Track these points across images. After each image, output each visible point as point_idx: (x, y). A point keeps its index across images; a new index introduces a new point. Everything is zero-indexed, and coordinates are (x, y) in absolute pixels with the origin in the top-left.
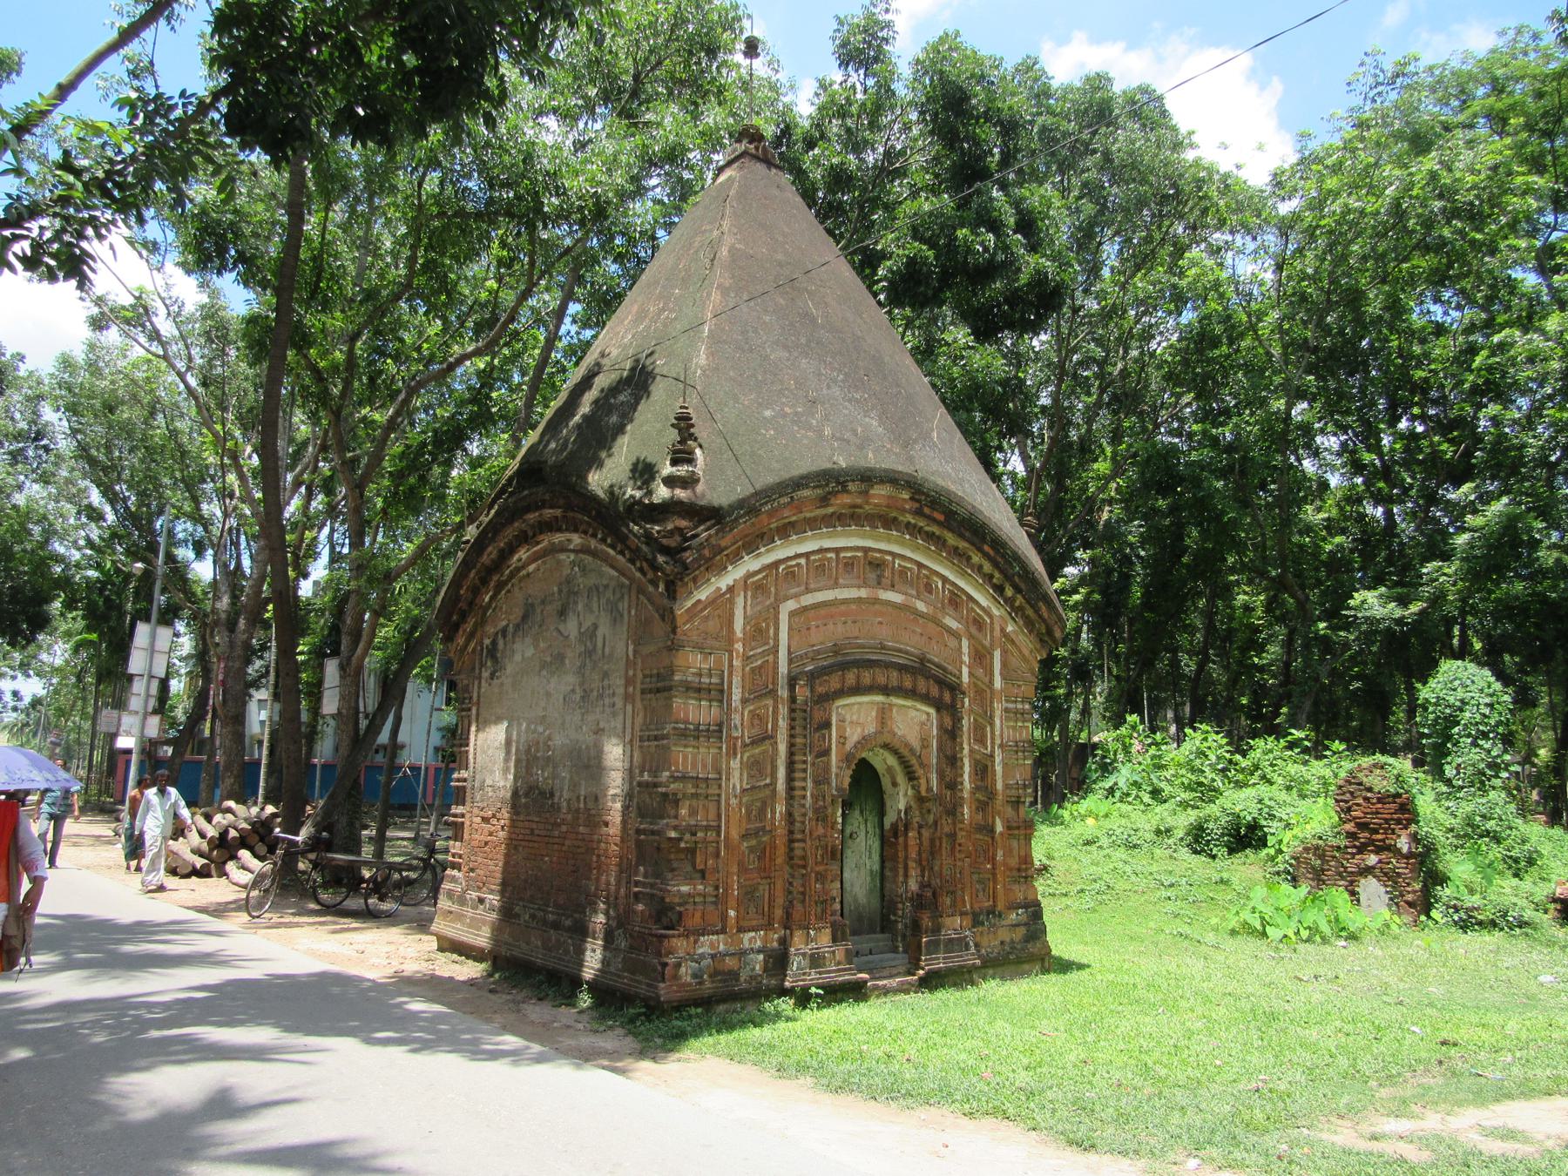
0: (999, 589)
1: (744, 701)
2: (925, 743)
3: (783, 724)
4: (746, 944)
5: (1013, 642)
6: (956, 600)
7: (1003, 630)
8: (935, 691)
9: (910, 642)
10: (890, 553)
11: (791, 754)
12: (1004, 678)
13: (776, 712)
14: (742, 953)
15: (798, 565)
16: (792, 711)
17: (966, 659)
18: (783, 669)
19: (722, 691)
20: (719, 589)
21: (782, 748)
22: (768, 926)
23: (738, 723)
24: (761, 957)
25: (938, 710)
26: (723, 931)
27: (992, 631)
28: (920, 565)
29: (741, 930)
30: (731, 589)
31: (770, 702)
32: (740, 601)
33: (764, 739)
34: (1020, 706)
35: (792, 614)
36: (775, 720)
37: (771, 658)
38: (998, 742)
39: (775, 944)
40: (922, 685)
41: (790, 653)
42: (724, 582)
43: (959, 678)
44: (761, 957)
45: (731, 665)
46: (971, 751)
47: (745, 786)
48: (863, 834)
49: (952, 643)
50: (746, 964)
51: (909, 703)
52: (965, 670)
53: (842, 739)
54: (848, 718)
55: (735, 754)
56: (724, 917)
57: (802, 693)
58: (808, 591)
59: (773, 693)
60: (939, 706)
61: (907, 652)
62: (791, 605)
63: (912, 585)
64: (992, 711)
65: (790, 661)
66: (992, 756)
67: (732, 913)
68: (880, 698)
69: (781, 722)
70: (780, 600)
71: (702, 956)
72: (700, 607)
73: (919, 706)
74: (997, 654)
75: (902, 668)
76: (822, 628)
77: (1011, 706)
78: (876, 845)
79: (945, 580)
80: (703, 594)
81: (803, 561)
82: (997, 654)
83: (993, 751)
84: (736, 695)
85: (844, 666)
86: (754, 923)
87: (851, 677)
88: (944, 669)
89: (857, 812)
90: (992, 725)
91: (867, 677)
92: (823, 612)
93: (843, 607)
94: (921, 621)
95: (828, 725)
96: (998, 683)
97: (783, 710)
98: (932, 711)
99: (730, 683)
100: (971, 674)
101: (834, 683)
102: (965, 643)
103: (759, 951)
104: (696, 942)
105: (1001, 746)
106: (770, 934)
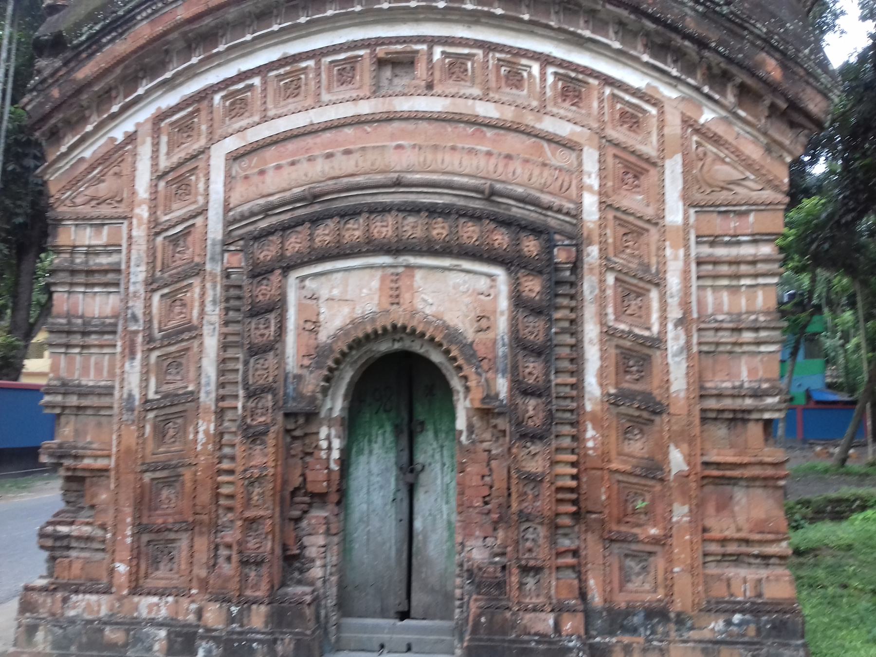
0: (661, 49)
1: (152, 284)
2: (483, 321)
3: (214, 314)
4: (144, 613)
5: (716, 140)
6: (573, 85)
7: (688, 122)
8: (501, 239)
9: (466, 163)
10: (420, 40)
11: (224, 346)
12: (689, 203)
13: (203, 295)
14: (133, 625)
15: (250, 87)
16: (227, 288)
17: (593, 181)
18: (215, 229)
19: (118, 271)
20: (113, 139)
21: (211, 343)
22: (179, 592)
23: (139, 311)
24: (163, 633)
25: (508, 269)
26: (107, 591)
27: (661, 128)
28: (488, 47)
29: (136, 590)
30: (131, 138)
31: (196, 281)
32: (145, 150)
33: (189, 329)
34: (747, 251)
35: (235, 157)
36: (202, 304)
37: (199, 221)
38: (675, 313)
39: (191, 618)
40: (470, 233)
41: (227, 209)
42: (118, 134)
43: (576, 215)
44: (163, 633)
45: (130, 237)
46: (608, 333)
47: (151, 395)
48: (438, 466)
49: (561, 158)
50: (138, 640)
51: (447, 262)
52: (590, 204)
53: (312, 326)
54: (324, 293)
55: (132, 355)
56: (112, 571)
57: (236, 260)
58: (265, 119)
59: (198, 270)
60: (510, 261)
61: (449, 186)
62: (232, 144)
63: (473, 83)
64: (663, 262)
65: (228, 223)
66: (658, 343)
67: (122, 568)
68: (386, 260)
69: (209, 308)
70: (212, 140)
71: (72, 621)
72: (84, 166)
73: (467, 265)
74: (673, 167)
75: (433, 211)
76: (287, 170)
77: (706, 250)
78: (453, 484)
79: (546, 60)
80: (88, 152)
81: (257, 81)
82: (673, 167)
83: (663, 331)
84: (139, 274)
85: (315, 220)
86: (162, 584)
87: (324, 234)
88: (536, 203)
89: (430, 434)
90: (659, 282)
91: (354, 231)
92: (291, 146)
93: (328, 135)
94: (489, 133)
95: (278, 306)
96: (675, 213)
97: (214, 291)
98: (500, 273)
99: (129, 259)
100: (605, 205)
101: (295, 243)
102: (590, 160)
103: (161, 625)
104: (65, 600)
105: (680, 322)
106: (185, 602)
